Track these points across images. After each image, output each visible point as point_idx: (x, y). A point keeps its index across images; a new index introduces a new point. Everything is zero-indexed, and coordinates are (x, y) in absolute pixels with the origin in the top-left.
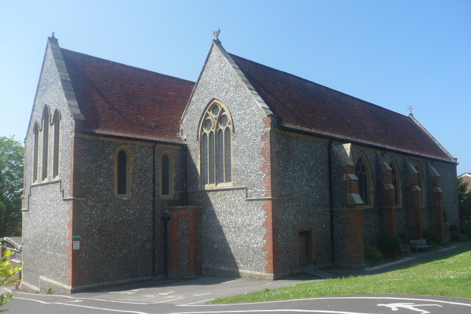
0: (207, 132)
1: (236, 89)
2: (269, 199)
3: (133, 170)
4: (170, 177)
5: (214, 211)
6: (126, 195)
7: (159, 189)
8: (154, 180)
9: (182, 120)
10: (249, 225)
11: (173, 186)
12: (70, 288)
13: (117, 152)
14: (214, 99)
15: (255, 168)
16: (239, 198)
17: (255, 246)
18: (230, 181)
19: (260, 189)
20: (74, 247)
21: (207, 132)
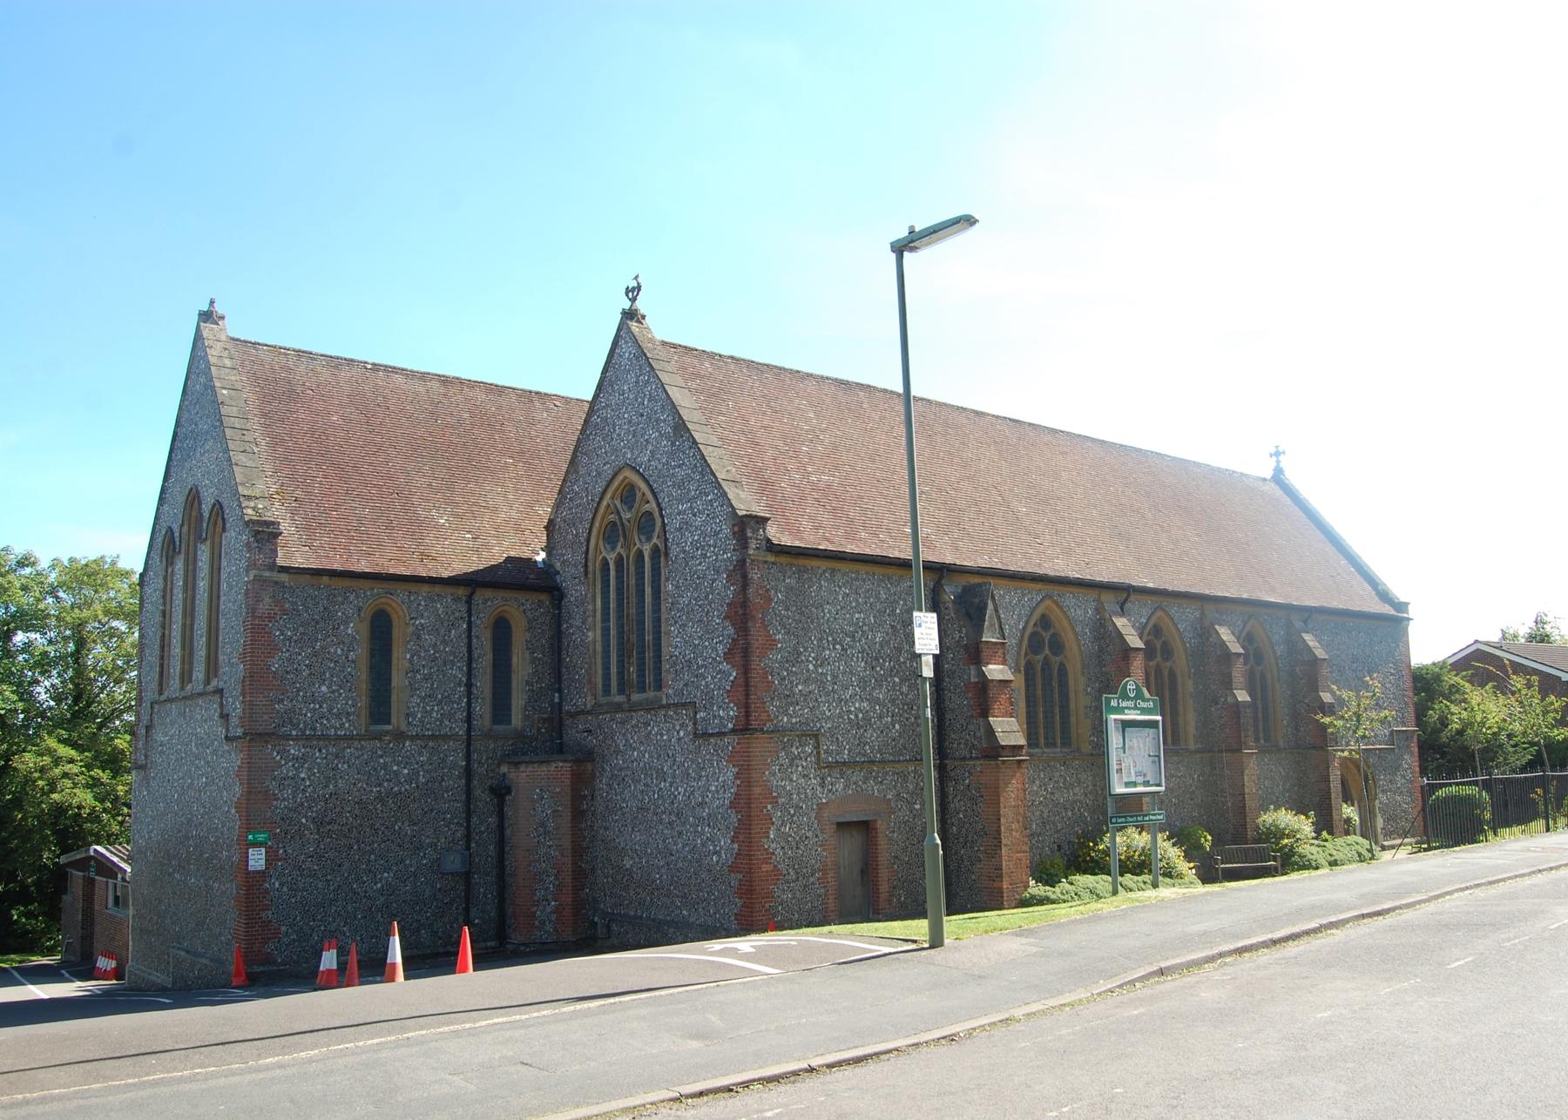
3: (411, 661)
7: (483, 709)
8: (469, 685)
10: (701, 804)
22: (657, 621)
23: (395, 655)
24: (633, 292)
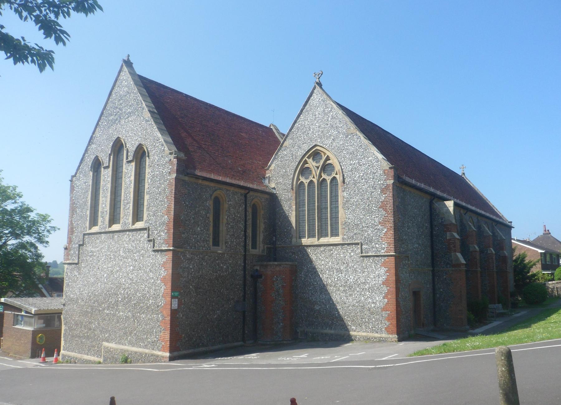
0: (304, 181)
1: (347, 137)
2: (391, 256)
4: (258, 229)
5: (314, 268)
6: (220, 248)
8: (245, 231)
9: (270, 166)
11: (261, 240)
12: (167, 354)
13: (213, 197)
14: (316, 146)
15: (373, 222)
16: (350, 254)
17: (373, 305)
18: (337, 235)
19: (379, 244)
20: (173, 305)
21: (306, 182)
23: (221, 216)
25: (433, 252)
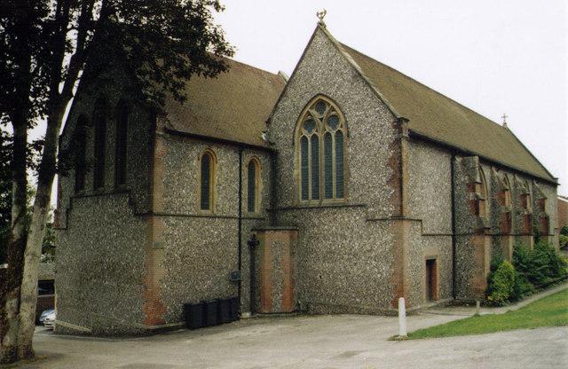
1: (352, 84)
7: (245, 204)
8: (240, 193)
17: (379, 276)
22: (341, 168)
24: (321, 15)
25: (453, 215)
